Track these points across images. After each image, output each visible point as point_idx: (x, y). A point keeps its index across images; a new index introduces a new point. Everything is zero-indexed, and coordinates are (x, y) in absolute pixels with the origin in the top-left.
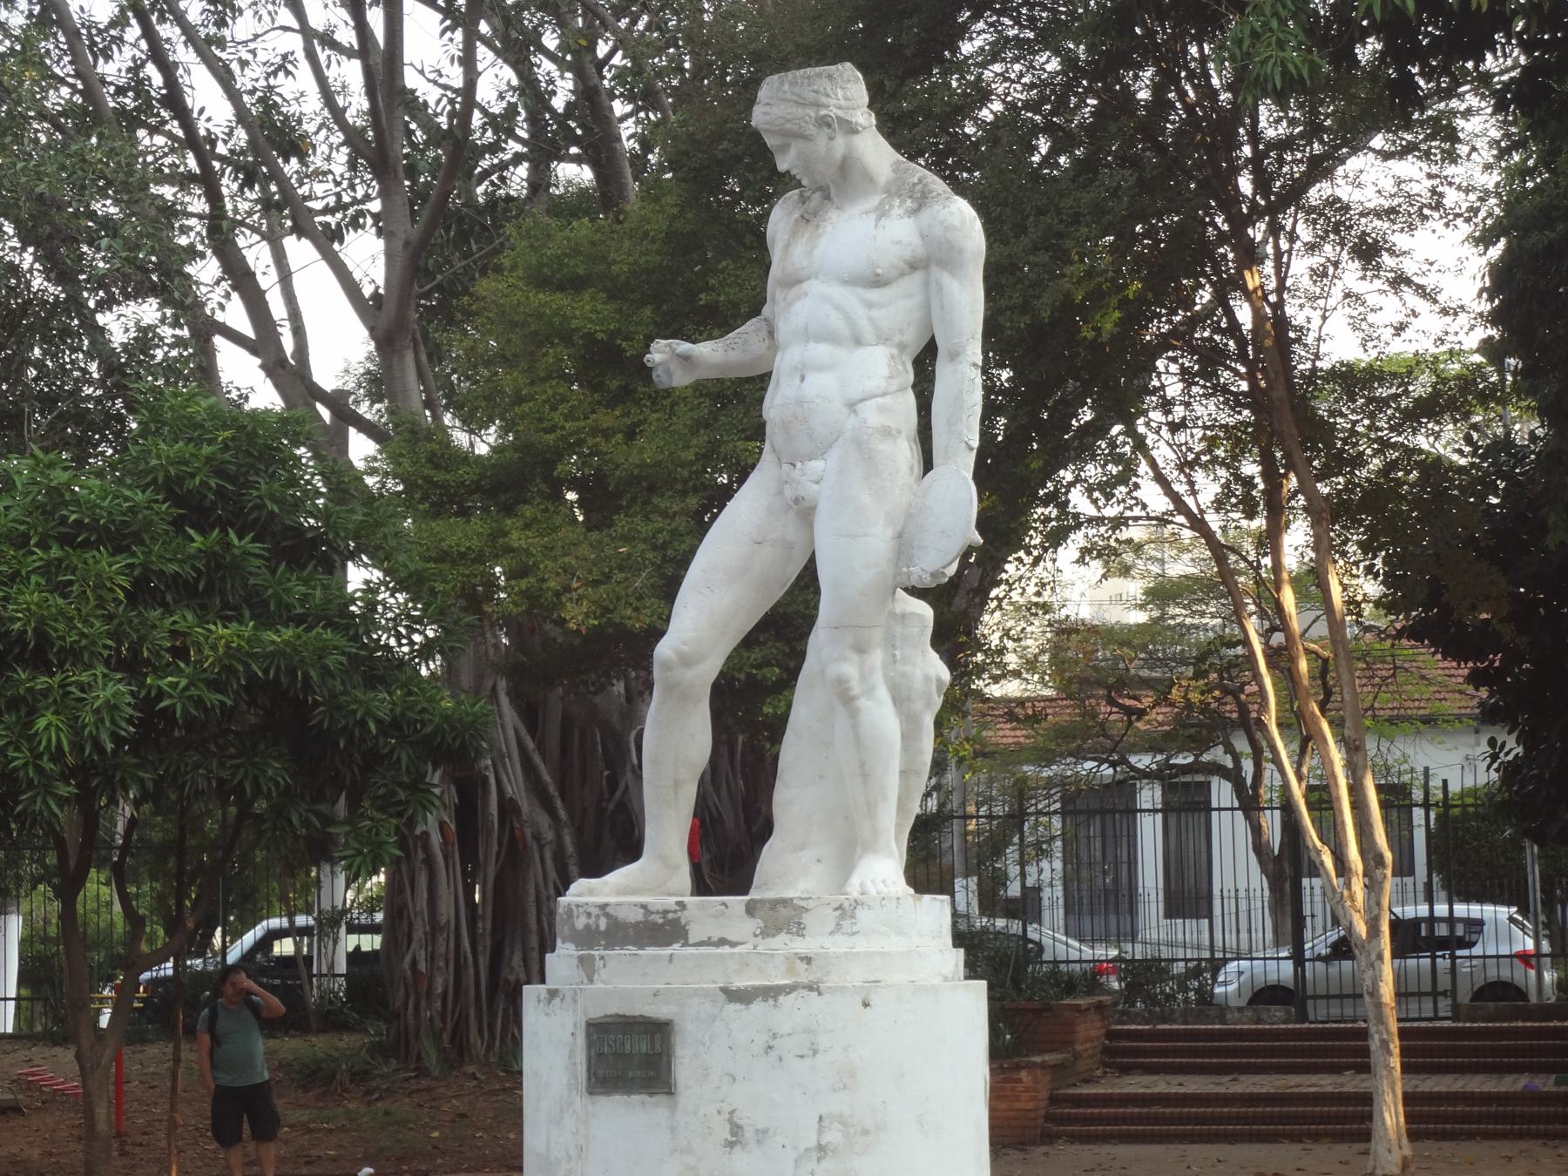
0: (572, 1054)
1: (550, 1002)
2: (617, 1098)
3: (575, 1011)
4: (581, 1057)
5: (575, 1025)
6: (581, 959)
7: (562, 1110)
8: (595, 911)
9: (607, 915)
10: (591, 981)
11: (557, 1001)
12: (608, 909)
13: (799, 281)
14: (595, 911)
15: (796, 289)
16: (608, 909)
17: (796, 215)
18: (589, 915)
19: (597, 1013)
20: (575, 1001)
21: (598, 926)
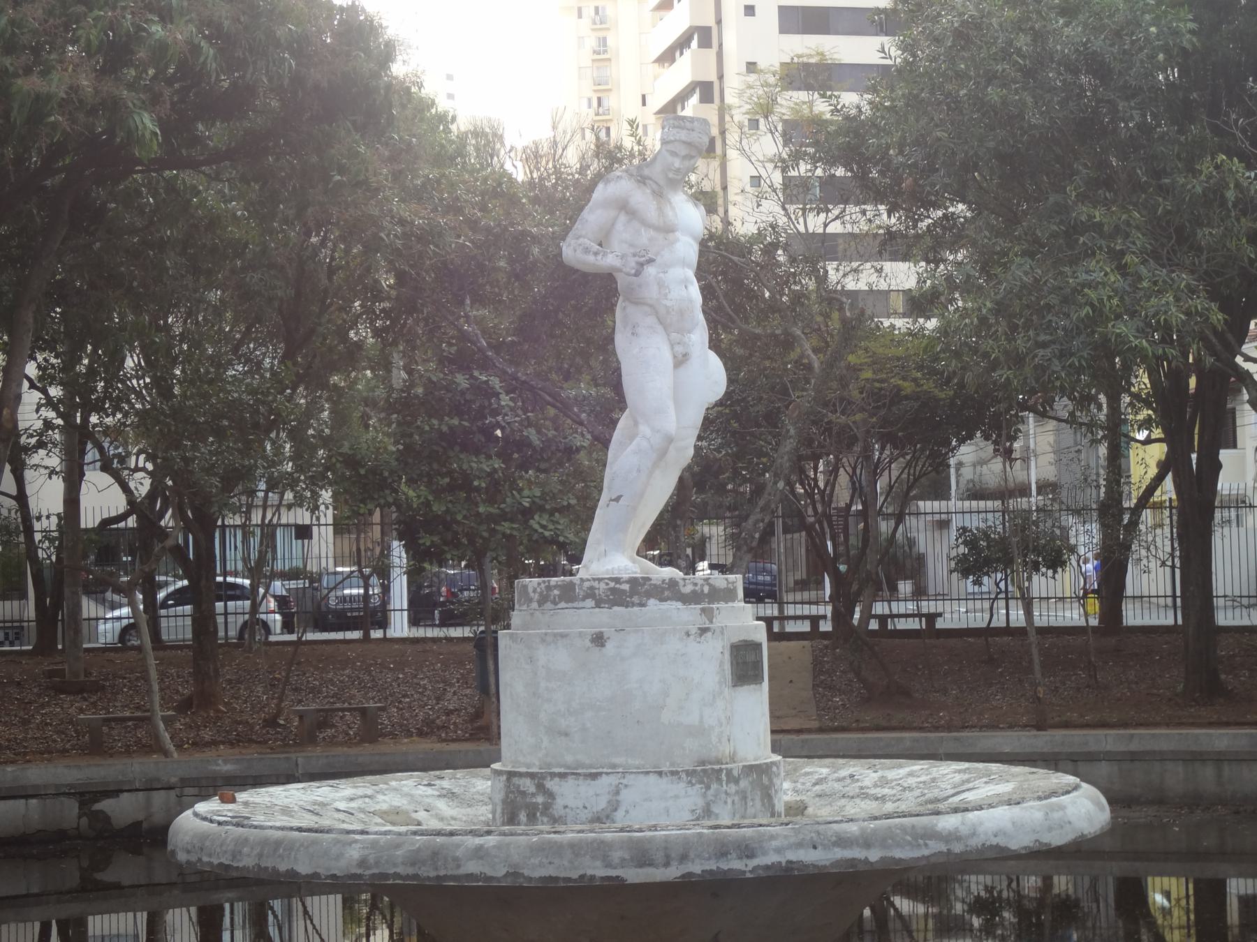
0: (721, 664)
1: (701, 635)
2: (745, 687)
3: (723, 639)
4: (727, 666)
5: (723, 647)
6: (703, 610)
7: (714, 696)
8: (702, 582)
9: (709, 584)
10: (711, 622)
11: (709, 634)
12: (710, 581)
13: (673, 231)
14: (702, 582)
15: (671, 236)
16: (710, 581)
17: (648, 191)
18: (696, 584)
19: (735, 640)
20: (722, 633)
21: (702, 591)
